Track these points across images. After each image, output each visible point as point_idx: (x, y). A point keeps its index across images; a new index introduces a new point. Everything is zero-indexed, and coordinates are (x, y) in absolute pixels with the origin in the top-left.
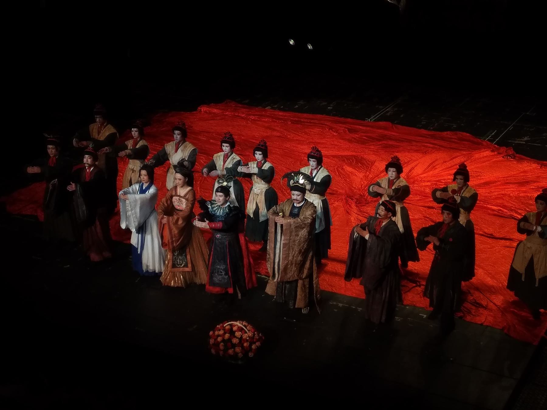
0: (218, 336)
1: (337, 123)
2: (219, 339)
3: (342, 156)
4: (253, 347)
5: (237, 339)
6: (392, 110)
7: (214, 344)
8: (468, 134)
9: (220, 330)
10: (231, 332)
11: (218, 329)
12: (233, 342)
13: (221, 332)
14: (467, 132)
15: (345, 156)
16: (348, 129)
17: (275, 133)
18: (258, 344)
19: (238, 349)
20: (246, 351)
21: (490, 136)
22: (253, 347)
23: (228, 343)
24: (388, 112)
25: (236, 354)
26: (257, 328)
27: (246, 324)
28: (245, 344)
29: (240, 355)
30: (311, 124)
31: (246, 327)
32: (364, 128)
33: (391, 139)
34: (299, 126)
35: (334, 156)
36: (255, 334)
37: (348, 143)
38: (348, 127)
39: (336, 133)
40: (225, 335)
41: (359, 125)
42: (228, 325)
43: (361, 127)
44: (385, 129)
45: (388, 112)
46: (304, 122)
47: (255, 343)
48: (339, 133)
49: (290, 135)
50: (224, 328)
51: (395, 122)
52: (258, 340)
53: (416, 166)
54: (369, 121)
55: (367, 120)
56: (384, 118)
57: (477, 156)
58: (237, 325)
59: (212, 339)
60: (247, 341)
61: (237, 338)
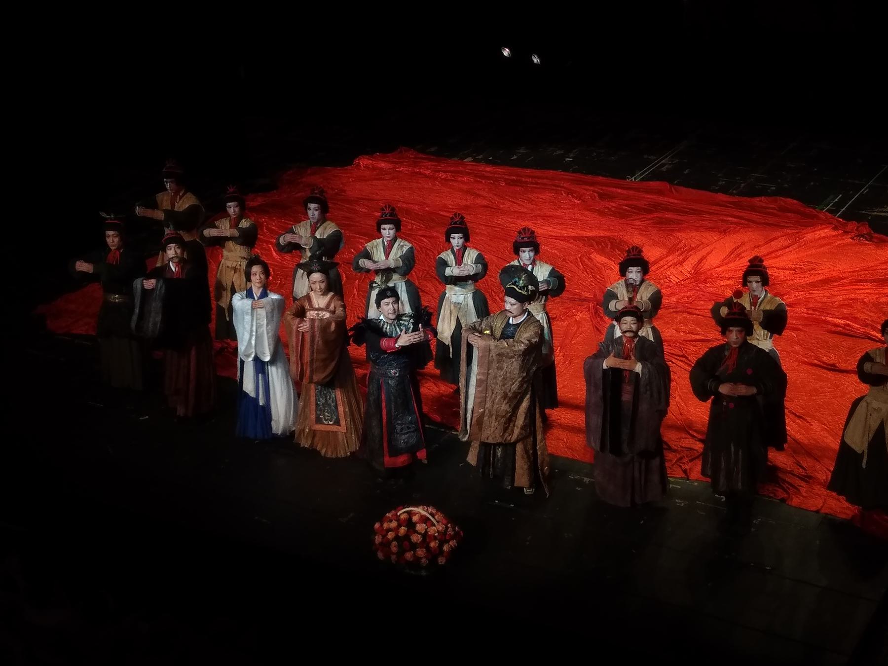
0: (389, 530)
1: (581, 184)
2: (390, 535)
3: (589, 238)
4: (446, 548)
5: (419, 536)
6: (670, 162)
7: (381, 544)
8: (795, 201)
9: (391, 521)
11: (388, 520)
12: (412, 541)
13: (394, 524)
14: (793, 198)
15: (593, 238)
16: (598, 193)
17: (479, 201)
18: (453, 543)
19: (421, 552)
20: (433, 555)
21: (831, 204)
22: (446, 548)
23: (404, 542)
24: (664, 165)
25: (417, 559)
26: (451, 517)
27: (434, 511)
28: (432, 544)
30: (538, 186)
31: (433, 517)
32: (625, 192)
33: (667, 210)
35: (575, 238)
36: (448, 528)
37: (598, 216)
38: (599, 191)
40: (399, 529)
41: (616, 187)
42: (404, 512)
43: (619, 191)
44: (660, 193)
45: (664, 165)
46: (526, 183)
47: (448, 542)
48: (583, 201)
49: (504, 204)
50: (398, 519)
52: (452, 538)
53: (708, 254)
54: (632, 180)
55: (629, 179)
56: (656, 176)
57: (809, 236)
58: (419, 513)
59: (378, 536)
60: (435, 538)
61: (420, 534)
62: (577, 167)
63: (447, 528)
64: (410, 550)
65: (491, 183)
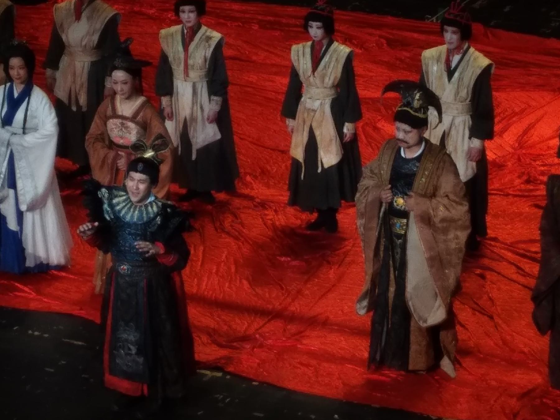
34: (277, 34)
37: (386, 71)
39: (361, 49)
43: (416, 35)
51: (492, 24)
54: (432, 21)
55: (428, 19)
62: (357, 3)
65: (239, 26)
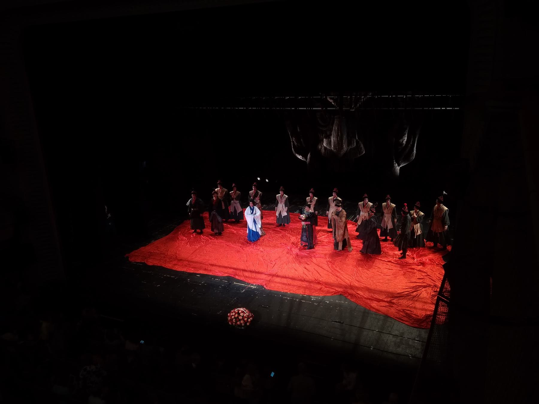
0: (232, 316)
2: (233, 317)
7: (230, 320)
9: (233, 313)
10: (239, 314)
13: (234, 314)
18: (251, 319)
19: (242, 322)
20: (245, 322)
23: (237, 319)
25: (241, 324)
26: (250, 311)
27: (245, 309)
28: (245, 319)
29: (243, 324)
47: (250, 318)
50: (235, 312)
52: (251, 317)
58: (241, 310)
60: (246, 317)
63: (249, 314)
64: (239, 321)
